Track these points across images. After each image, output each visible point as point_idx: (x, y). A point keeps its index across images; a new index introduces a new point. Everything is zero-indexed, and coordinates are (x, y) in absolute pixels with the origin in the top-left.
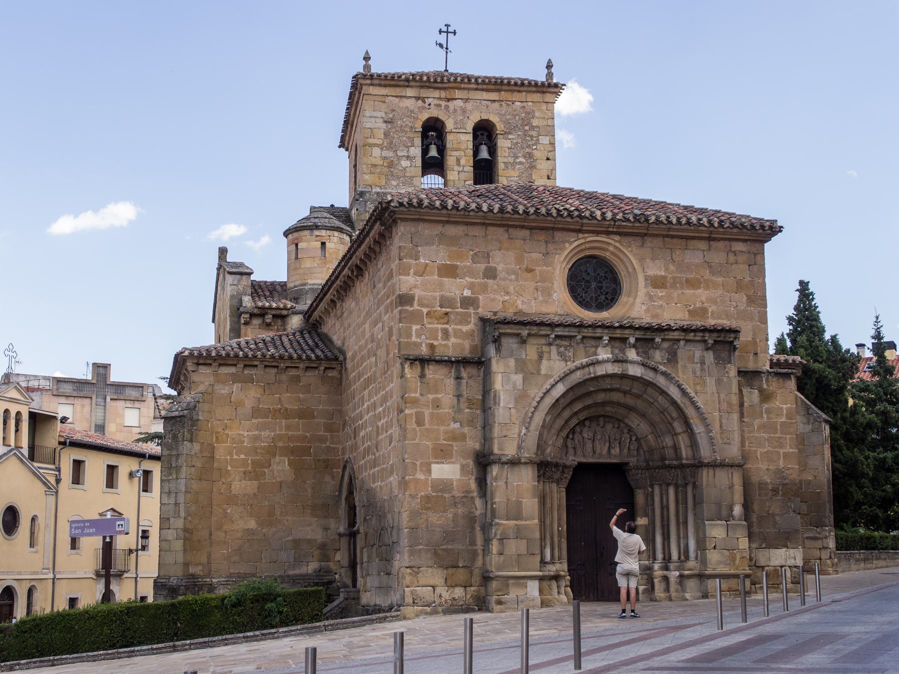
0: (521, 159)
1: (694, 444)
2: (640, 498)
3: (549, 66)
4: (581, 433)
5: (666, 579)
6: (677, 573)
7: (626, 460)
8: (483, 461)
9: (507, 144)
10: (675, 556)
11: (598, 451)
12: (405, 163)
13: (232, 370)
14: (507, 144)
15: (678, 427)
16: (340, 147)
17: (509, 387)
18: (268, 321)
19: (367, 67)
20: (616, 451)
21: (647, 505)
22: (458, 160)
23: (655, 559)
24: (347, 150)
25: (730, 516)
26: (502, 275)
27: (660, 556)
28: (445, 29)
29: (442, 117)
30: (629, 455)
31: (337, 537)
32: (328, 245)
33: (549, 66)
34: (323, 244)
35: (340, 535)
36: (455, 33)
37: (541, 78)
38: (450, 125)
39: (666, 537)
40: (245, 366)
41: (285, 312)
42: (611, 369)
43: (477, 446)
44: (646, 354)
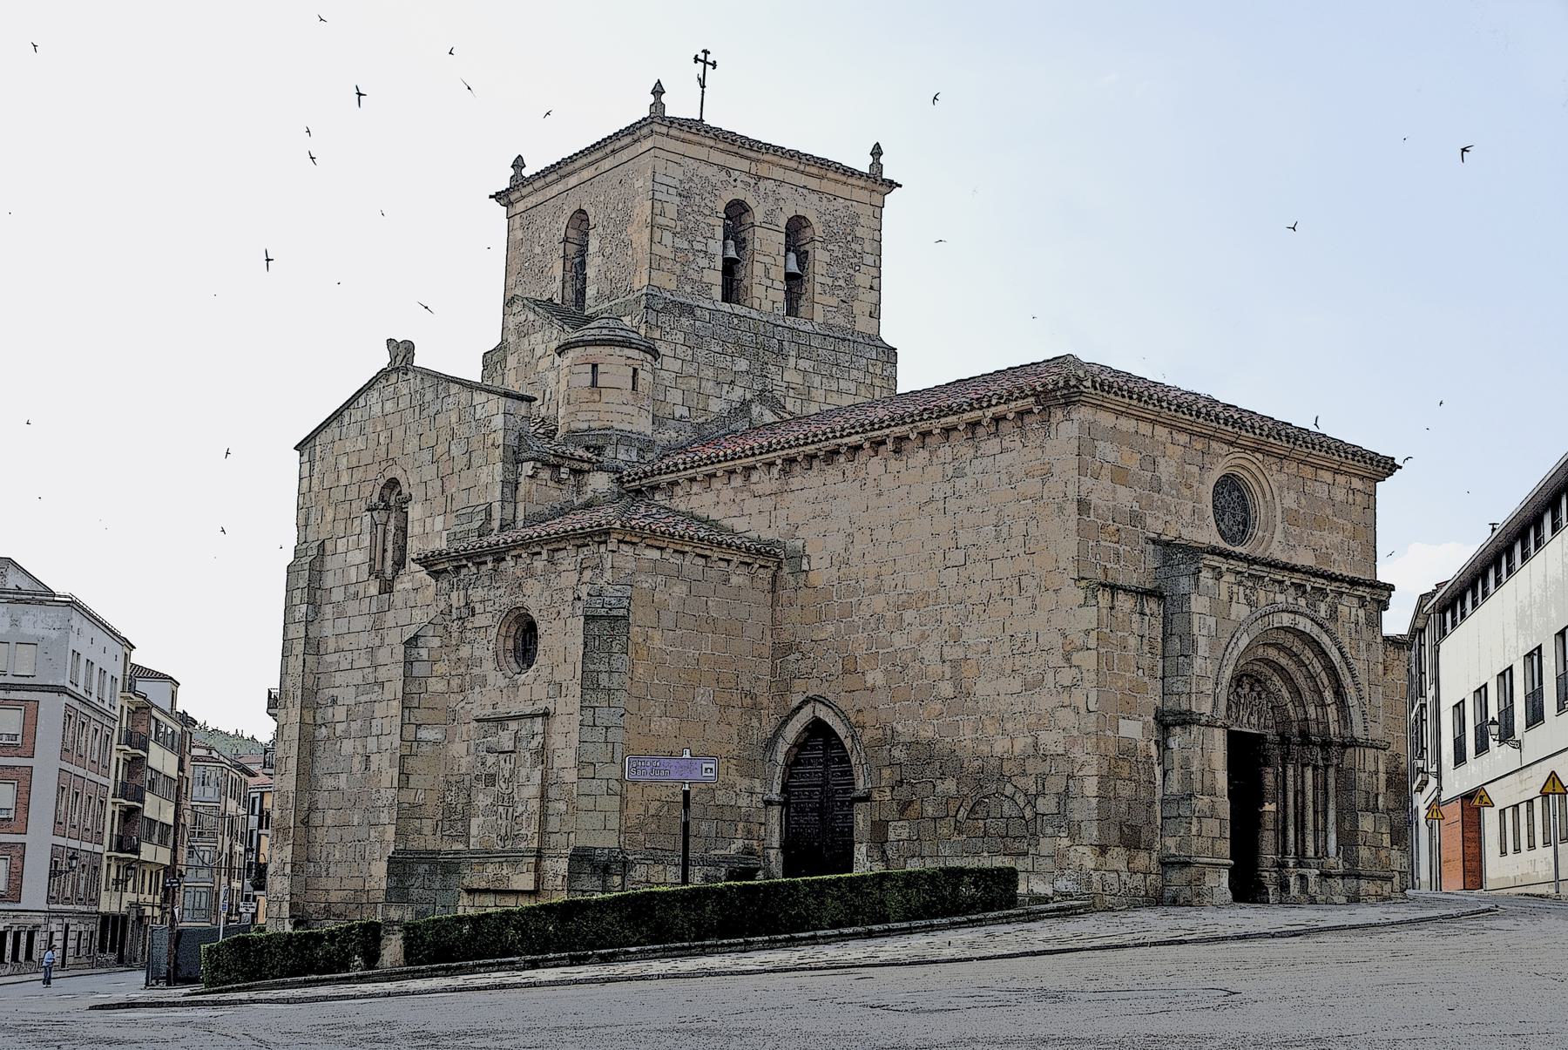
0: (841, 282)
1: (1345, 719)
2: (1269, 779)
3: (877, 152)
5: (1303, 877)
7: (1263, 731)
8: (1168, 722)
9: (826, 257)
10: (1310, 852)
12: (703, 263)
13: (656, 554)
14: (826, 257)
15: (1329, 696)
16: (497, 196)
17: (1204, 632)
18: (564, 476)
19: (658, 106)
20: (1254, 720)
22: (767, 270)
23: (1285, 853)
24: (509, 204)
25: (1375, 809)
26: (1166, 488)
28: (701, 56)
29: (751, 202)
31: (761, 805)
32: (641, 374)
33: (877, 152)
34: (635, 370)
35: (768, 803)
36: (714, 65)
37: (863, 164)
38: (758, 215)
39: (1300, 827)
40: (675, 551)
41: (586, 466)
42: (1286, 620)
43: (1159, 703)
44: (1312, 605)
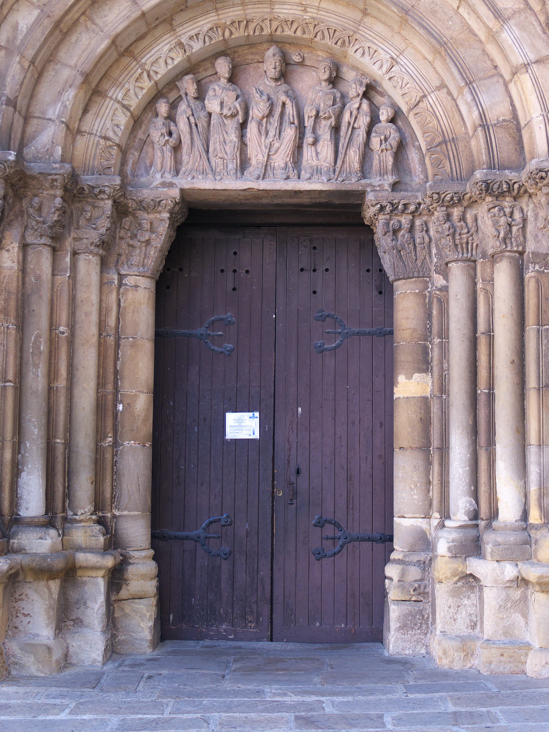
4: (200, 97)
6: (510, 571)
7: (353, 184)
11: (256, 154)
21: (427, 335)
27: (460, 504)
30: (364, 172)
39: (481, 436)
